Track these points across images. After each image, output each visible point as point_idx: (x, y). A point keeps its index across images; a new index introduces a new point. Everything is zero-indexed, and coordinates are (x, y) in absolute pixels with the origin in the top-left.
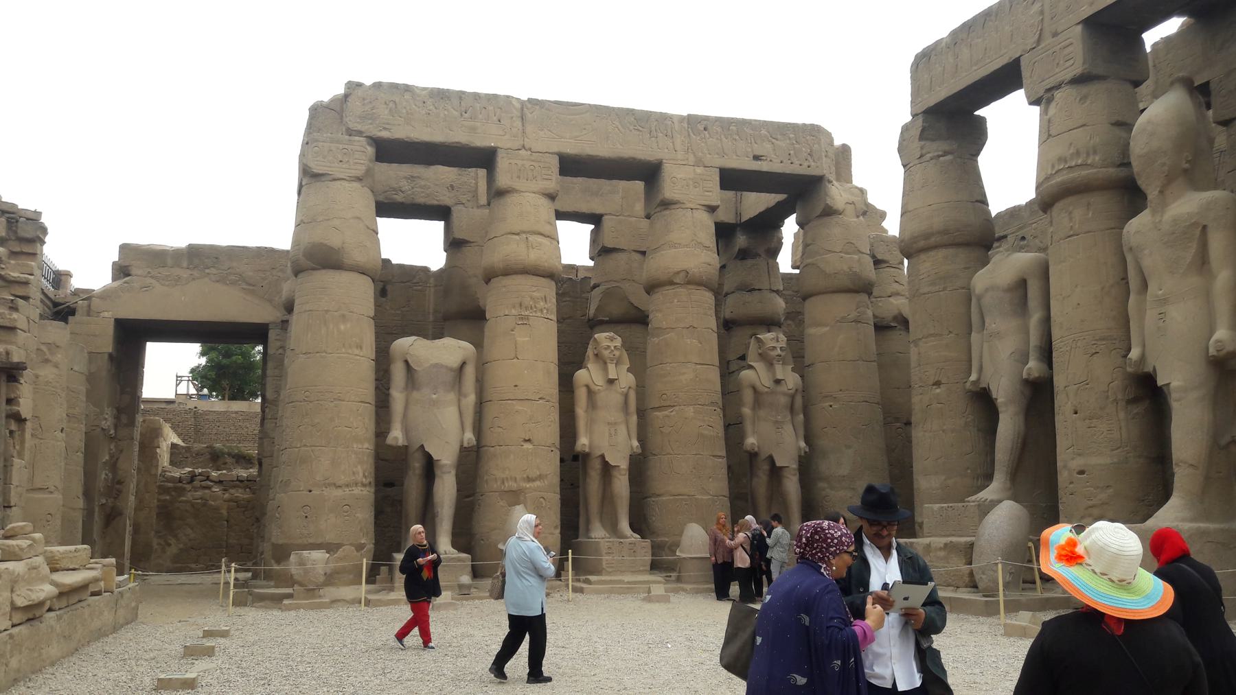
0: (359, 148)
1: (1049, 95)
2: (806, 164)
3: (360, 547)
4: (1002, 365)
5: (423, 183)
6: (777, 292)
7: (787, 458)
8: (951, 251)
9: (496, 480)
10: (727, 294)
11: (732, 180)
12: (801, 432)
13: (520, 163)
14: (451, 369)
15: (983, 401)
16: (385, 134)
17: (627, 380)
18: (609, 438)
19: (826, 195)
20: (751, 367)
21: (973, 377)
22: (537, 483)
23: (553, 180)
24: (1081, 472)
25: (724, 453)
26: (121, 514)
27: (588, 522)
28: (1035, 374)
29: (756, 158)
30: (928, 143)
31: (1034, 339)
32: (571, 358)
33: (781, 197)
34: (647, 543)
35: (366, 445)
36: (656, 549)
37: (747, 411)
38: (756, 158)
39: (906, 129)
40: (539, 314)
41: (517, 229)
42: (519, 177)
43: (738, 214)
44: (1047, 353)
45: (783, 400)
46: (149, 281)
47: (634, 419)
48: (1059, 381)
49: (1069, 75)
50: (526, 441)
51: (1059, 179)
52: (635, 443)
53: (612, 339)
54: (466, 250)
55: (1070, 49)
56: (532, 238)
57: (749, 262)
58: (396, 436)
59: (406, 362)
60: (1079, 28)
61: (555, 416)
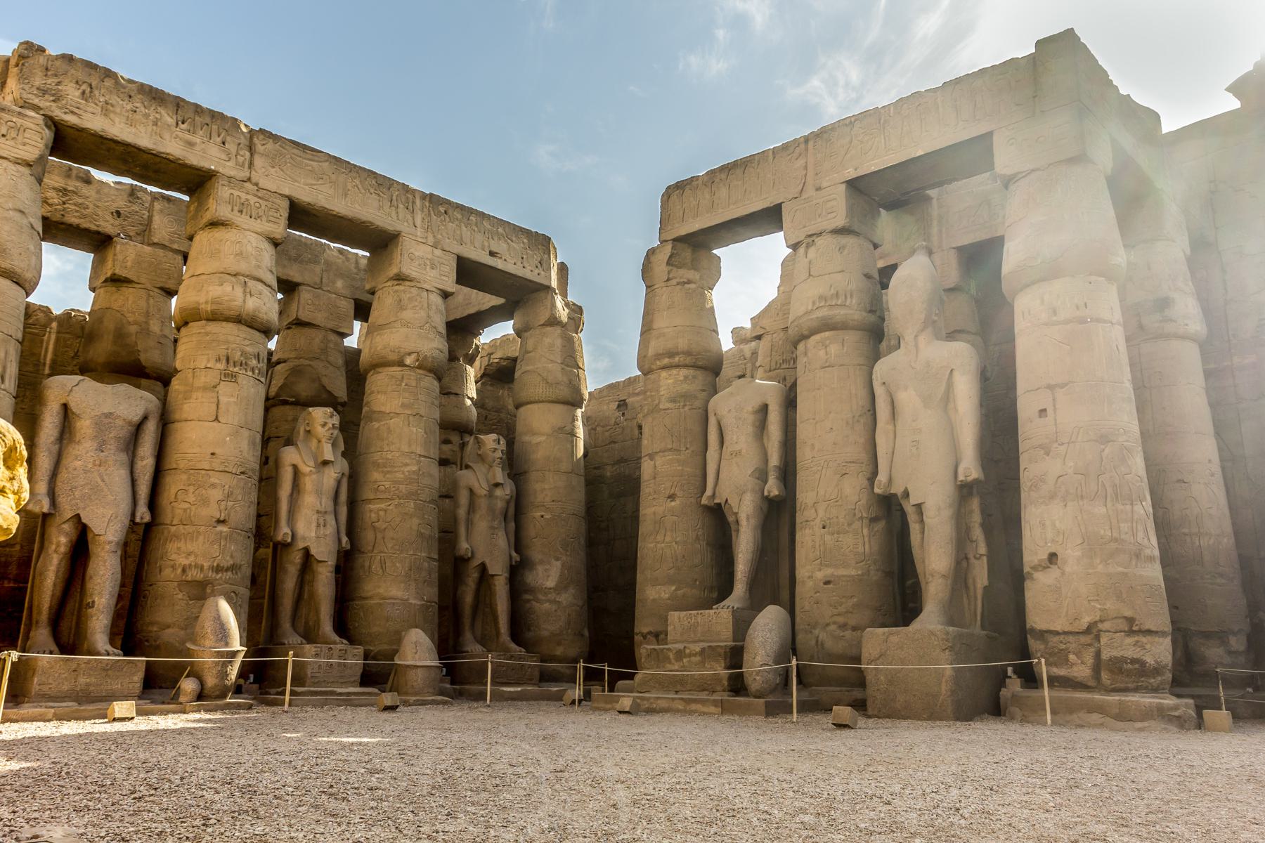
0: (33, 126)
1: (810, 240)
2: (537, 271)
4: (738, 482)
5: (80, 201)
8: (690, 372)
9: (173, 567)
11: (468, 272)
20: (467, 467)
21: (709, 492)
23: (279, 228)
24: (827, 583)
25: (436, 557)
28: (775, 492)
29: (492, 254)
31: (774, 460)
33: (499, 301)
38: (492, 254)
40: (250, 373)
42: (241, 212)
44: (788, 472)
45: (500, 505)
47: (343, 511)
48: (805, 496)
49: (830, 228)
50: (219, 522)
51: (819, 314)
52: (345, 539)
55: (834, 203)
56: (251, 283)
59: (65, 407)
60: (844, 186)
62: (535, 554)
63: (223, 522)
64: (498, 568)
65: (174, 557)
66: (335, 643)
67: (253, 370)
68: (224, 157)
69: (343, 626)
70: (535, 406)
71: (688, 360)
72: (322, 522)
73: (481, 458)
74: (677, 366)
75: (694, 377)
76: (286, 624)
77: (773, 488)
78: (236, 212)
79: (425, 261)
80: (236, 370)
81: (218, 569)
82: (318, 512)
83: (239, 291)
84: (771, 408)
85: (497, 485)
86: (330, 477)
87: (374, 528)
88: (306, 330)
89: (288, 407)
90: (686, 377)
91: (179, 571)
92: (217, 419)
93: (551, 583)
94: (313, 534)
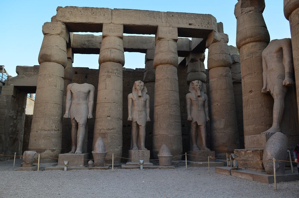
2: (207, 26)
3: (53, 150)
6: (203, 72)
7: (201, 122)
10: (188, 73)
11: (182, 32)
12: (207, 113)
13: (110, 27)
15: (268, 95)
16: (68, 21)
18: (138, 116)
19: (214, 35)
20: (190, 92)
21: (264, 88)
26: (18, 140)
27: (133, 145)
28: (288, 83)
29: (190, 24)
30: (244, 8)
31: (287, 70)
32: (127, 89)
35: (57, 117)
37: (188, 107)
38: (190, 24)
39: (236, 6)
40: (114, 74)
43: (190, 48)
45: (201, 103)
46: (23, 75)
47: (148, 110)
53: (140, 83)
56: (112, 50)
57: (194, 63)
61: (120, 109)
62: (215, 117)
63: (109, 116)
65: (98, 127)
68: (104, 19)
70: (213, 69)
71: (252, 39)
72: (140, 113)
73: (194, 88)
74: (248, 43)
75: (255, 45)
77: (287, 81)
79: (168, 32)
81: (109, 129)
82: (139, 111)
83: (109, 52)
84: (283, 49)
85: (199, 96)
86: (141, 101)
87: (157, 114)
89: (147, 83)
90: (252, 46)
91: (99, 130)
92: (106, 89)
93: (222, 126)
94: (138, 118)
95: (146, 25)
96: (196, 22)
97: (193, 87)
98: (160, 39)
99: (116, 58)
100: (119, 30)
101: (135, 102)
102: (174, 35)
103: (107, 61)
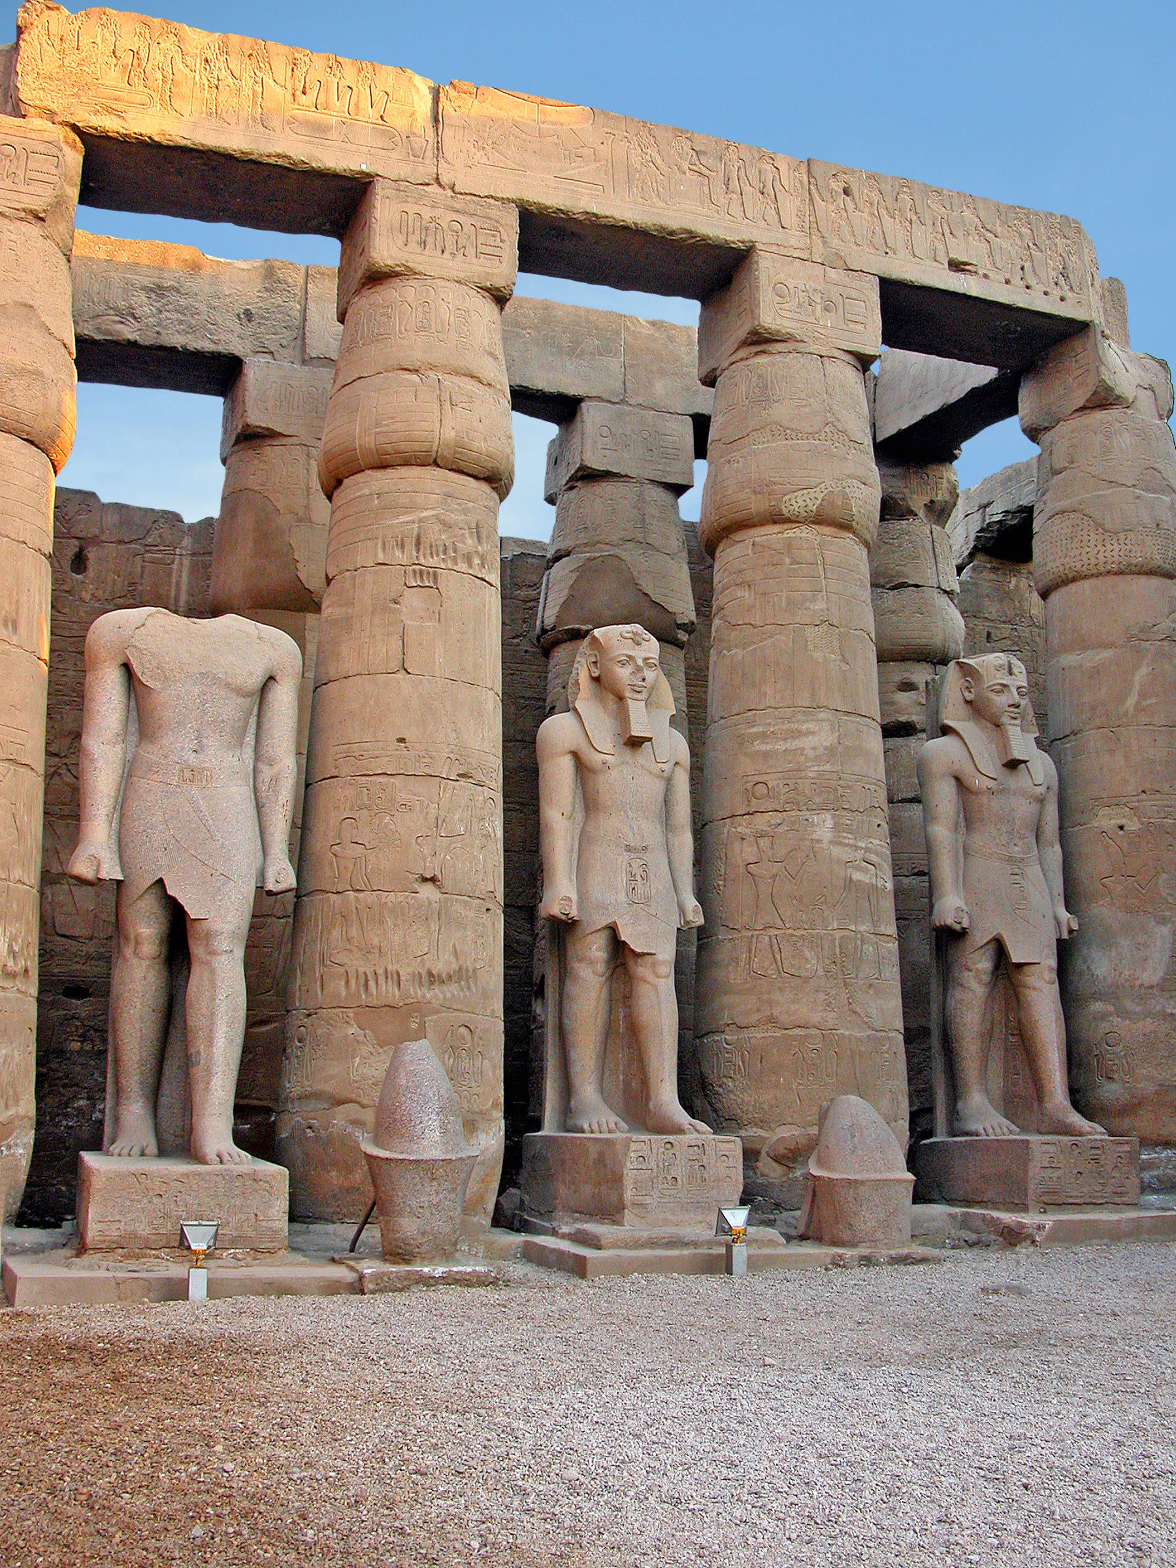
5: (183, 302)
6: (949, 593)
13: (427, 213)
14: (240, 692)
17: (673, 746)
20: (946, 730)
22: (452, 989)
29: (956, 266)
33: (984, 374)
34: (732, 1146)
36: (750, 1156)
37: (942, 832)
38: (956, 266)
40: (462, 566)
41: (416, 356)
42: (424, 244)
45: (1024, 809)
47: (685, 842)
52: (691, 903)
54: (271, 452)
56: (449, 381)
58: (97, 855)
59: (127, 667)
63: (433, 880)
64: (1034, 950)
66: (680, 1131)
67: (468, 559)
69: (697, 1091)
70: (1086, 584)
76: (588, 1090)
78: (413, 246)
79: (814, 299)
80: (432, 562)
81: (433, 978)
88: (606, 488)
94: (622, 897)
95: (672, 233)
96: (991, 254)
97: (969, 697)
98: (768, 341)
99: (475, 445)
100: (491, 241)
101: (601, 778)
102: (860, 327)
103: (407, 463)
